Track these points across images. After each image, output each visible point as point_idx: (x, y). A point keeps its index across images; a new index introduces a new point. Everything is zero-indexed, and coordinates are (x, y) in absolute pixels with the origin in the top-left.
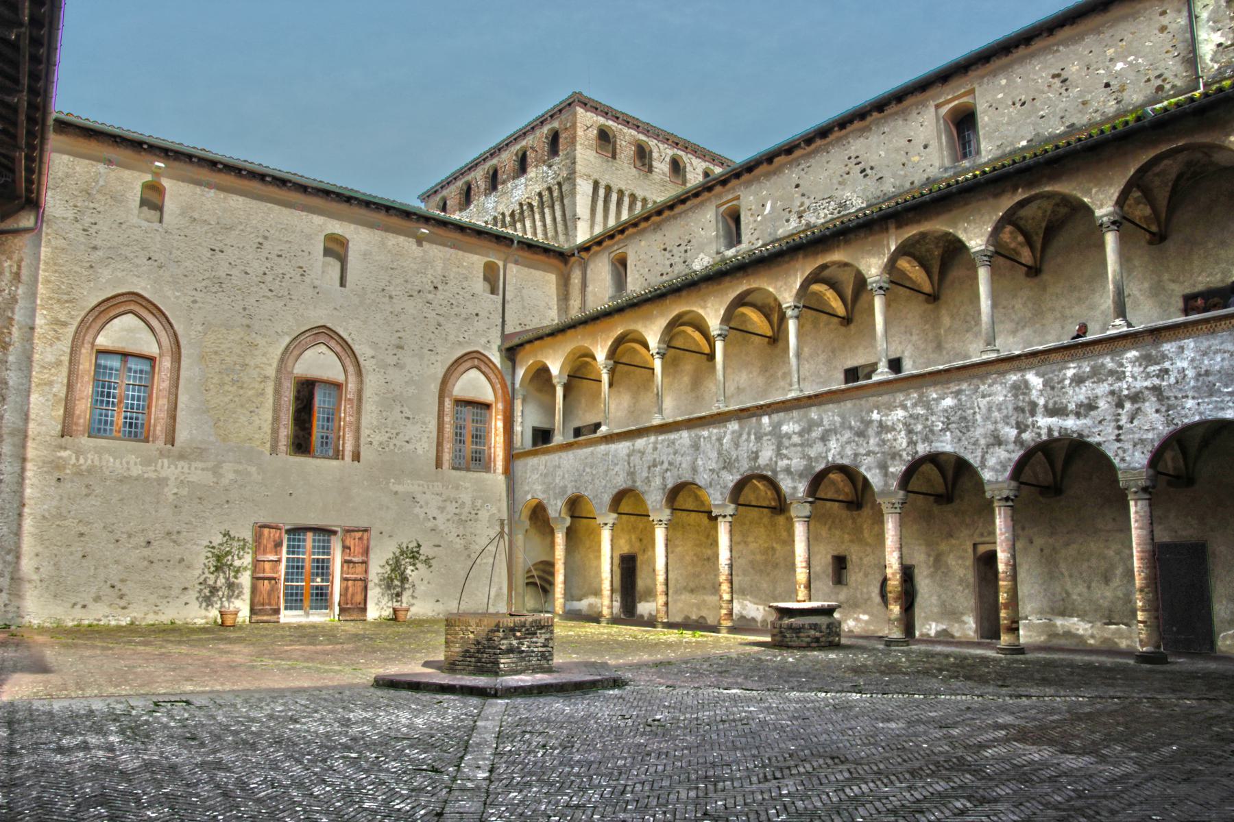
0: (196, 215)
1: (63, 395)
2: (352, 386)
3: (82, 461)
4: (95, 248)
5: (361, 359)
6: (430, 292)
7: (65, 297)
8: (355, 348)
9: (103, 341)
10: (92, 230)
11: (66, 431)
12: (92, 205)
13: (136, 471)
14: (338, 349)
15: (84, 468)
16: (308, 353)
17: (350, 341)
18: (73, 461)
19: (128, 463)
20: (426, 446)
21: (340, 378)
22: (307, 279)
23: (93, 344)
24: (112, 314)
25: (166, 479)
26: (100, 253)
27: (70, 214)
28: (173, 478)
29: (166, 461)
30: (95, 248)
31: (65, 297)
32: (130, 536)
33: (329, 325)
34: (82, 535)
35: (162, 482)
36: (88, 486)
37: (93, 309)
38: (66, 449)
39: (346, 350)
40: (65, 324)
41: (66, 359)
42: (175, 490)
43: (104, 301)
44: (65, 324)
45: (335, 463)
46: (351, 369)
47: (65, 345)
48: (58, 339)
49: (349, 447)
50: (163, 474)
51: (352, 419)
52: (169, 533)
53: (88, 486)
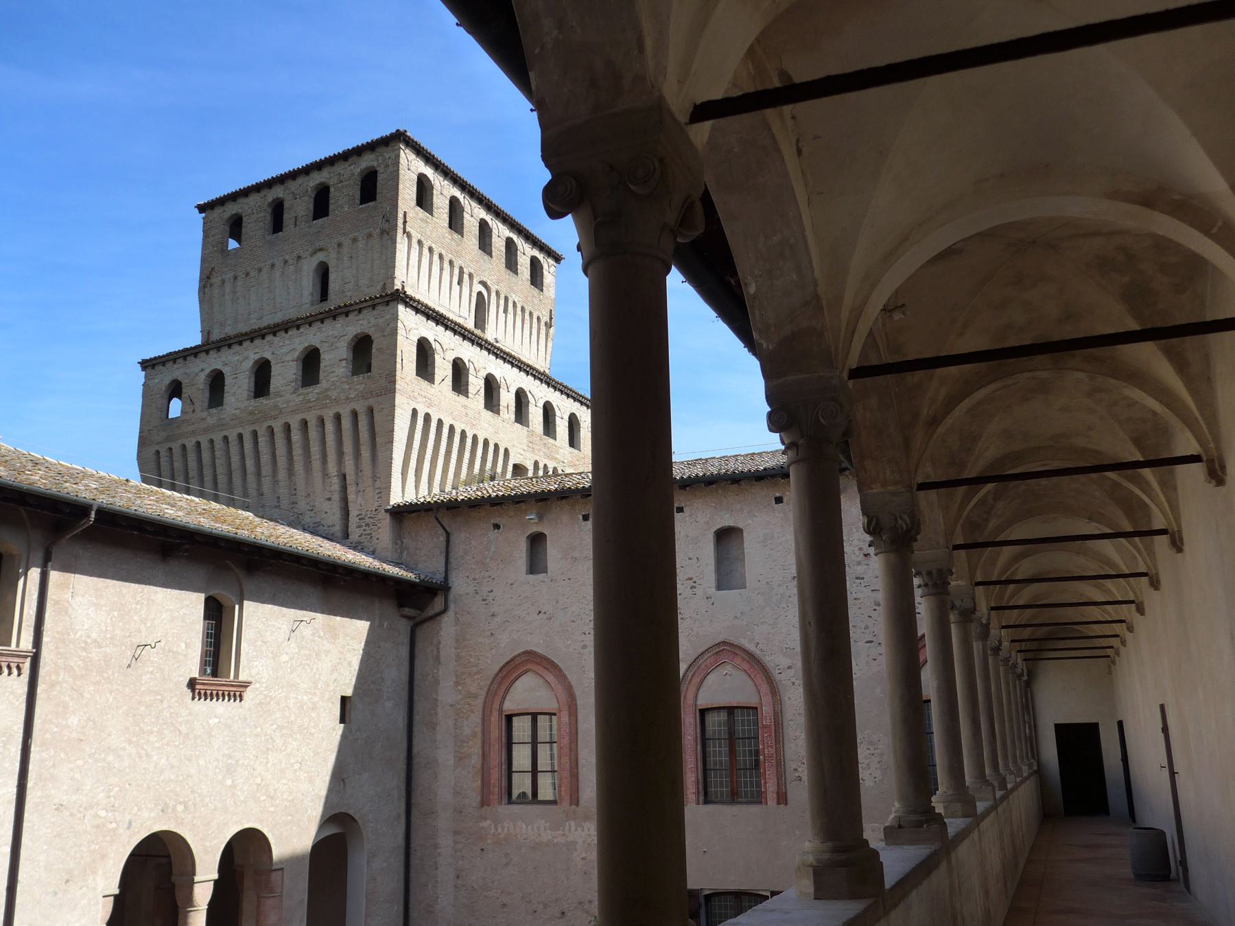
0: (576, 554)
1: (479, 766)
2: (767, 710)
3: (500, 830)
4: (493, 615)
5: (775, 672)
6: (859, 563)
7: (474, 669)
8: (768, 660)
9: (509, 706)
10: (490, 599)
11: (484, 802)
12: (487, 574)
13: (546, 836)
14: (746, 666)
15: (502, 836)
16: (711, 678)
17: (757, 652)
18: (493, 830)
19: (538, 829)
20: (878, 774)
21: (753, 701)
22: (699, 591)
23: (501, 711)
24: (515, 675)
25: (575, 843)
26: (498, 619)
27: (471, 590)
28: (580, 841)
29: (572, 823)
30: (493, 615)
31: (474, 669)
32: (545, 907)
33: (731, 639)
34: (504, 905)
35: (571, 846)
36: (506, 855)
37: (497, 675)
38: (486, 819)
39: (755, 664)
40: (475, 696)
41: (479, 729)
42: (584, 855)
43: (504, 666)
44: (475, 696)
45: (754, 809)
46: (765, 687)
47: (476, 718)
48: (472, 711)
49: (771, 788)
50: (571, 838)
51: (773, 751)
52: (580, 903)
53: (506, 855)
